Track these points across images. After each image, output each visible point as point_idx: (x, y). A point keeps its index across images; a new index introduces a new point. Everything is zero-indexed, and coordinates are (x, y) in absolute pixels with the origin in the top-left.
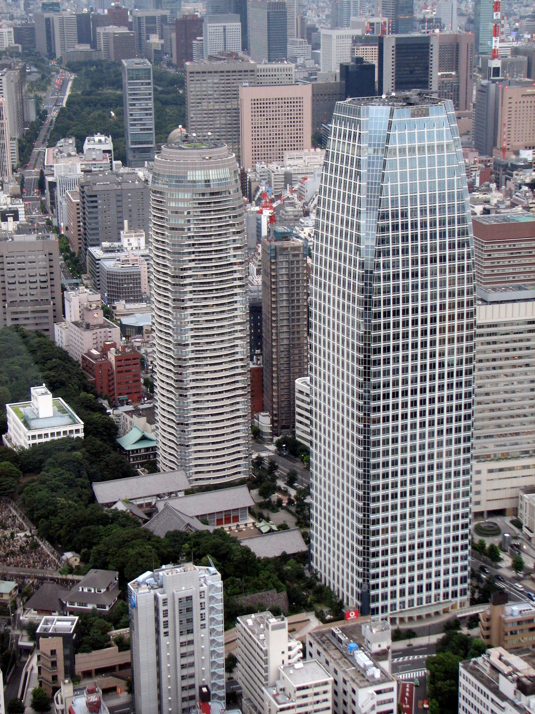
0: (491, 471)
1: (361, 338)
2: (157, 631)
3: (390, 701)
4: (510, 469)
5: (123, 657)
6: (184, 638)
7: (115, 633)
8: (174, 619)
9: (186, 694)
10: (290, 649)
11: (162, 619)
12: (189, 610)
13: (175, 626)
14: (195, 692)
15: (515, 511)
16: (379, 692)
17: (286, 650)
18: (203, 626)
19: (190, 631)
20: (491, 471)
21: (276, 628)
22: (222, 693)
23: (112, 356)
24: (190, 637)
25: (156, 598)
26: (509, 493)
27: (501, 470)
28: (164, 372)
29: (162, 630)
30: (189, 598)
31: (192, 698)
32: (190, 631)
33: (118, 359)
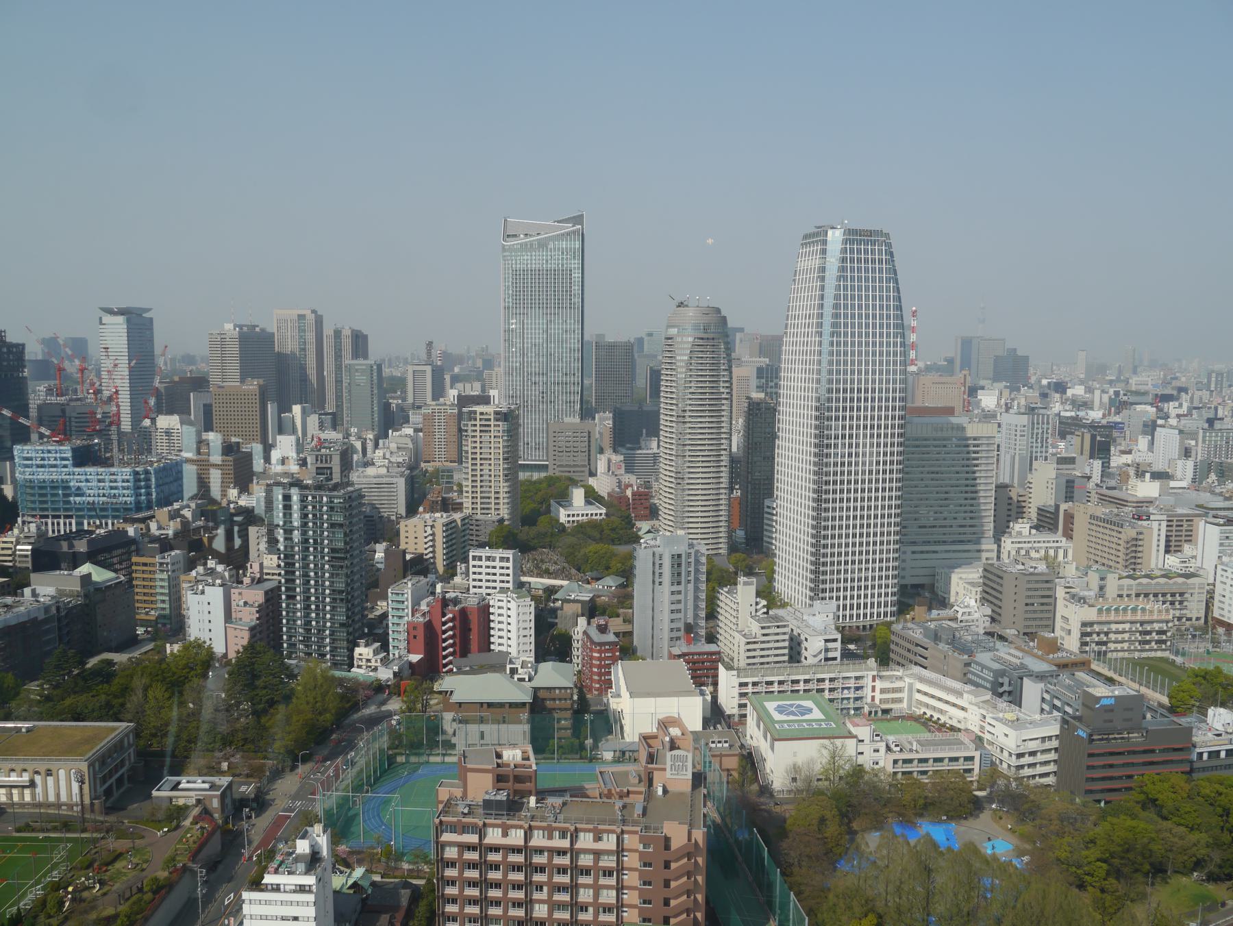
0: (913, 552)
1: (815, 473)
2: (654, 582)
3: (836, 649)
5: (627, 628)
6: (675, 588)
7: (621, 611)
8: (667, 570)
9: (674, 625)
10: (757, 604)
11: (657, 571)
12: (679, 565)
13: (667, 578)
14: (681, 625)
15: (933, 585)
16: (827, 641)
18: (689, 581)
20: (913, 552)
21: (745, 584)
22: (703, 632)
23: (629, 493)
27: (922, 552)
29: (657, 580)
30: (679, 556)
31: (678, 630)
32: (679, 583)
33: (634, 494)
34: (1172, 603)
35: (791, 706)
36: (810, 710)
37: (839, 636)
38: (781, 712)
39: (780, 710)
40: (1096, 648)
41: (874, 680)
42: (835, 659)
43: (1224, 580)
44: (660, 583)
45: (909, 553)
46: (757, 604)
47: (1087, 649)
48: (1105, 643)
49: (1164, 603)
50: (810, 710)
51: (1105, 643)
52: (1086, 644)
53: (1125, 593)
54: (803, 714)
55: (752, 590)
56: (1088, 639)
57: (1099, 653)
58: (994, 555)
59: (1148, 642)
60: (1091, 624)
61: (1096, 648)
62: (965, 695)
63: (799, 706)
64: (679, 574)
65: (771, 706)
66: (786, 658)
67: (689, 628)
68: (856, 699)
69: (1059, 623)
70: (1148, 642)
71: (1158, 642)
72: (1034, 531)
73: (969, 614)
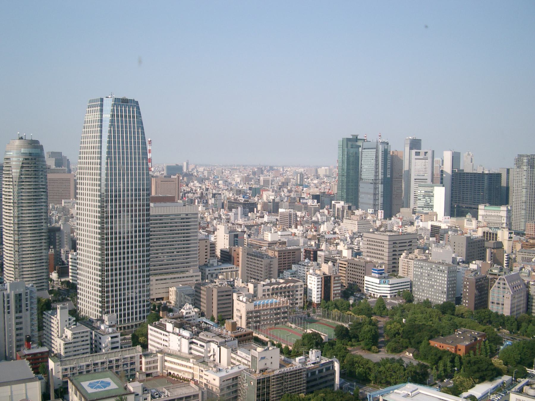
0: (157, 280)
4: (165, 279)
6: (18, 315)
10: (70, 320)
12: (20, 300)
14: (23, 337)
17: (68, 320)
18: (27, 310)
19: (21, 312)
20: (157, 280)
24: (20, 315)
25: (4, 294)
26: (165, 290)
27: (162, 280)
28: (8, 258)
30: (20, 295)
32: (21, 312)
34: (289, 296)
35: (98, 382)
36: (109, 384)
37: (119, 334)
38: (92, 387)
39: (91, 386)
40: (254, 325)
41: (141, 358)
42: (117, 347)
43: (311, 282)
44: (9, 313)
45: (154, 280)
46: (70, 320)
47: (250, 325)
48: (259, 322)
49: (285, 297)
50: (109, 384)
51: (259, 322)
52: (249, 323)
53: (266, 293)
54: (105, 387)
55: (67, 311)
56: (250, 320)
57: (256, 327)
58: (200, 278)
59: (279, 318)
60: (251, 312)
61: (254, 325)
62: (191, 360)
63: (102, 382)
64: (21, 306)
65: (85, 385)
66: (89, 350)
67: (29, 340)
68: (131, 370)
69: (235, 313)
70: (279, 318)
71: (283, 318)
72: (220, 263)
73: (190, 313)
